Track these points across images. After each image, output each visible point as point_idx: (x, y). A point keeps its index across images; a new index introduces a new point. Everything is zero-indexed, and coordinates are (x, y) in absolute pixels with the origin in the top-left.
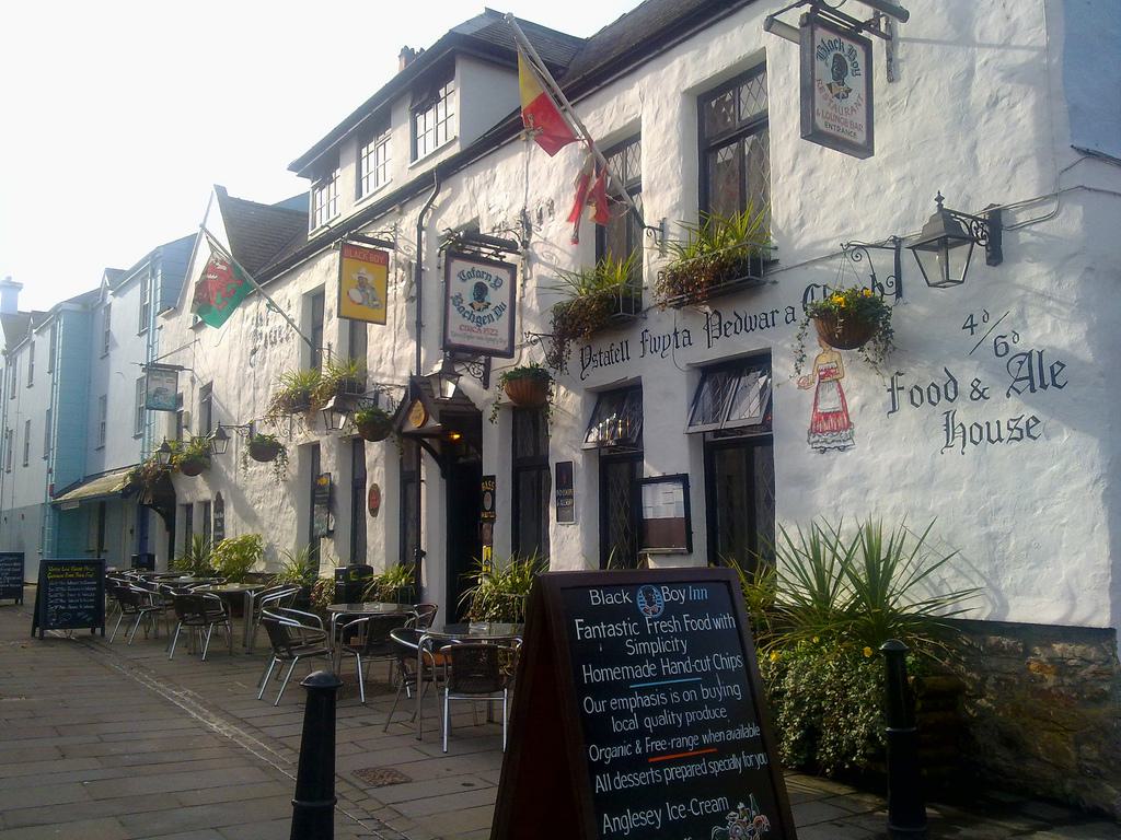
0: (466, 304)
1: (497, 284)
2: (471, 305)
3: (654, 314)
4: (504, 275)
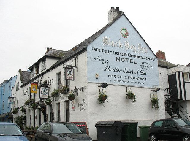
0: (42, 93)
1: (47, 90)
4: (48, 88)
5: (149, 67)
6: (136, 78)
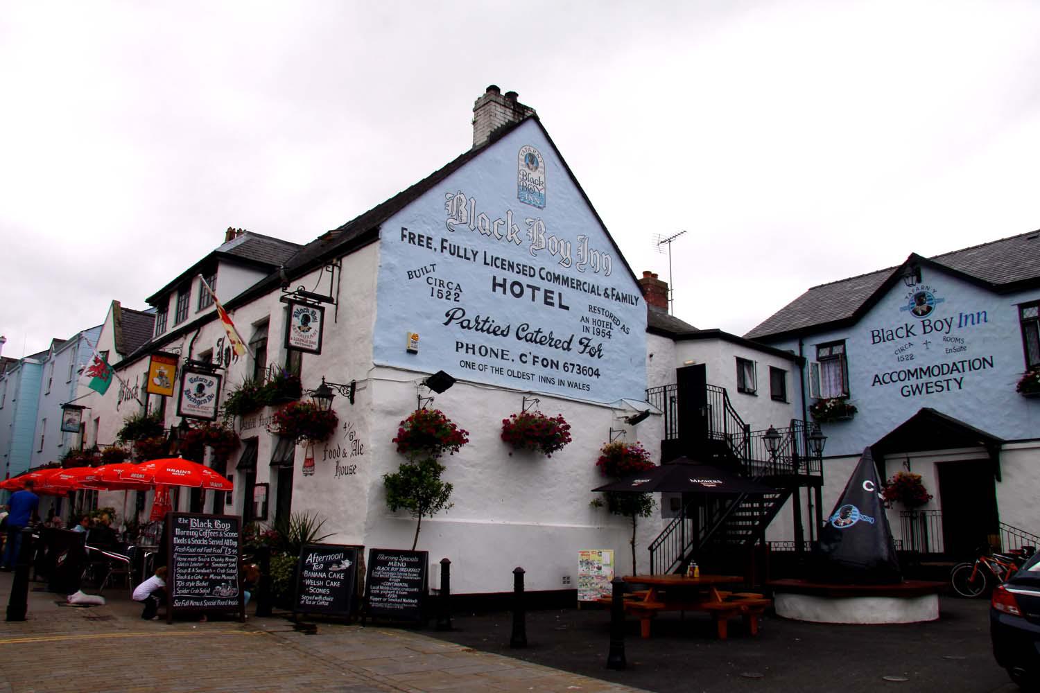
1: (210, 384)
2: (195, 395)
4: (215, 380)
5: (613, 325)
6: (561, 365)
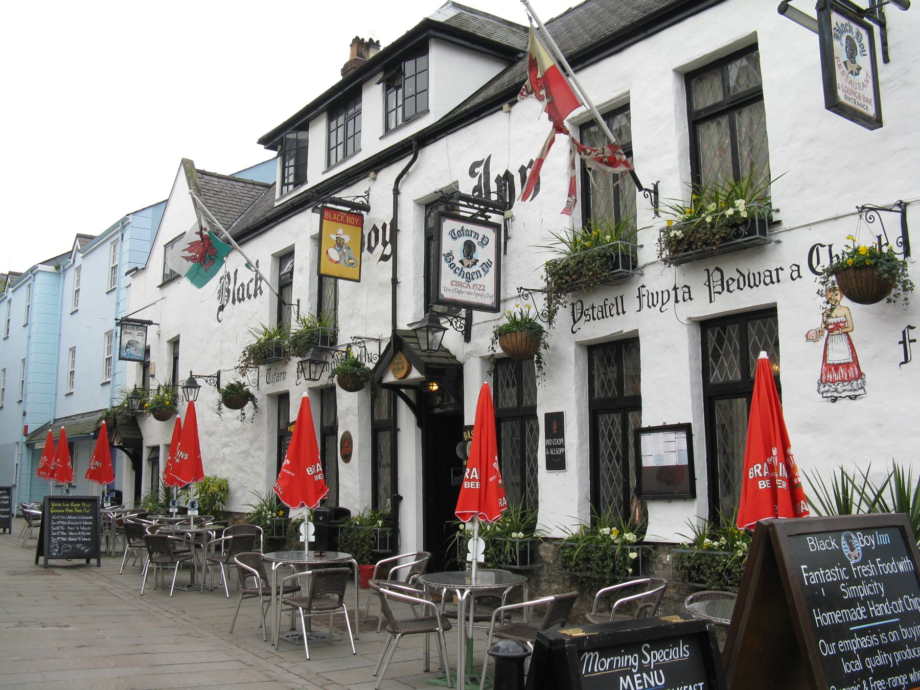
0: (456, 261)
1: (484, 242)
2: (461, 262)
3: (649, 273)
4: (490, 234)
